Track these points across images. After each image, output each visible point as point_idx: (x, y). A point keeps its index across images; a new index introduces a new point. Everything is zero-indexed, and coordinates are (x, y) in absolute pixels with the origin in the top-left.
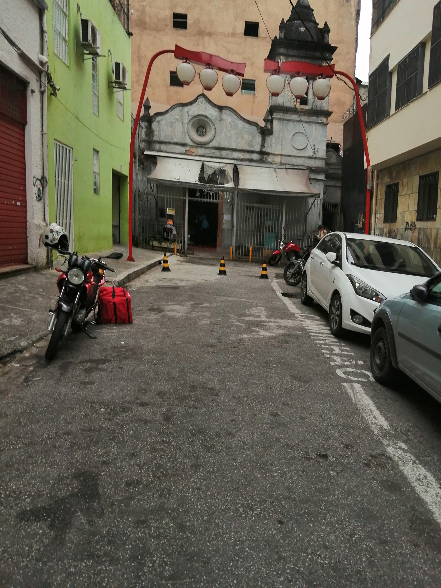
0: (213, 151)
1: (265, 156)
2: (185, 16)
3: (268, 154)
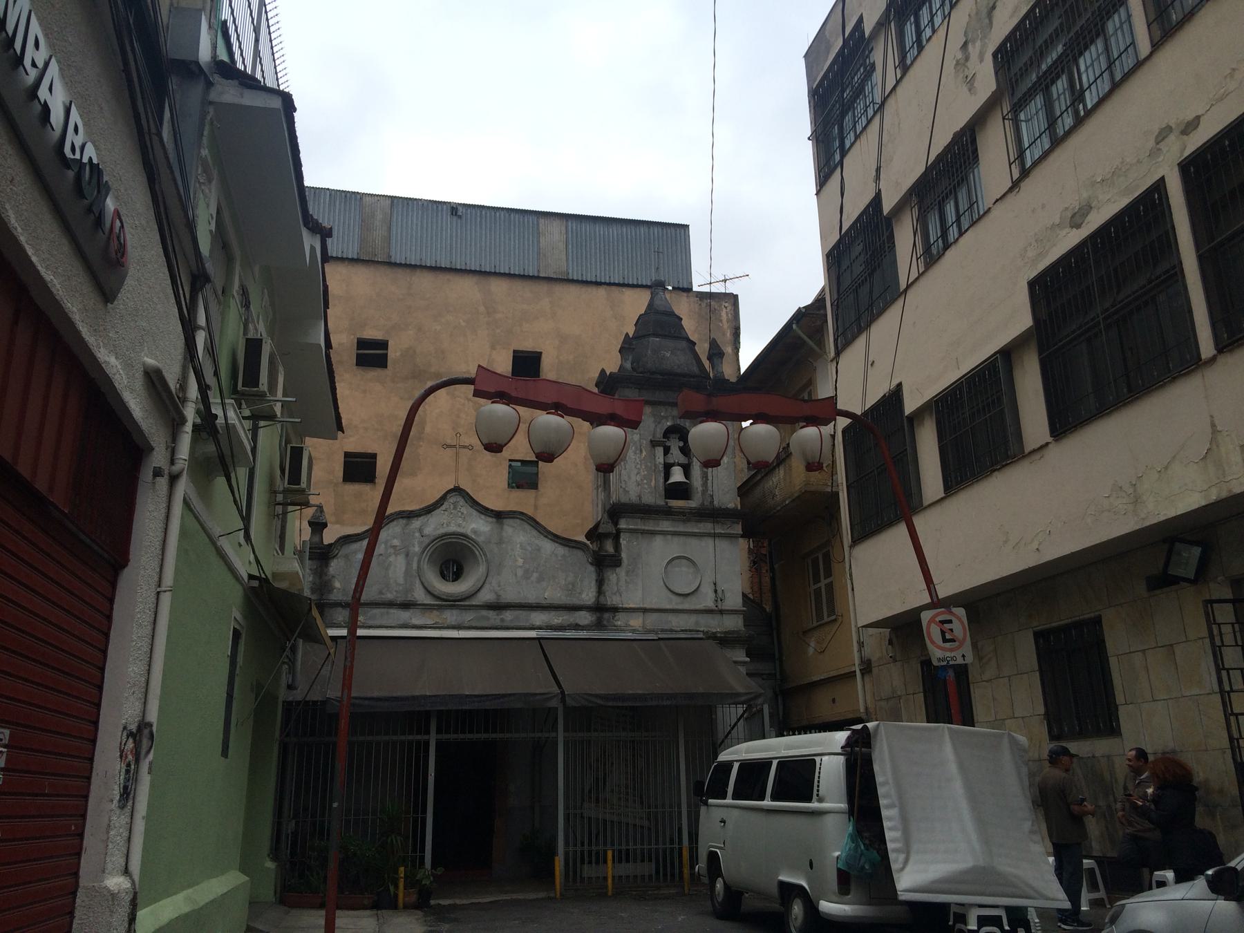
0: (484, 613)
1: (606, 615)
2: (383, 345)
3: (615, 610)
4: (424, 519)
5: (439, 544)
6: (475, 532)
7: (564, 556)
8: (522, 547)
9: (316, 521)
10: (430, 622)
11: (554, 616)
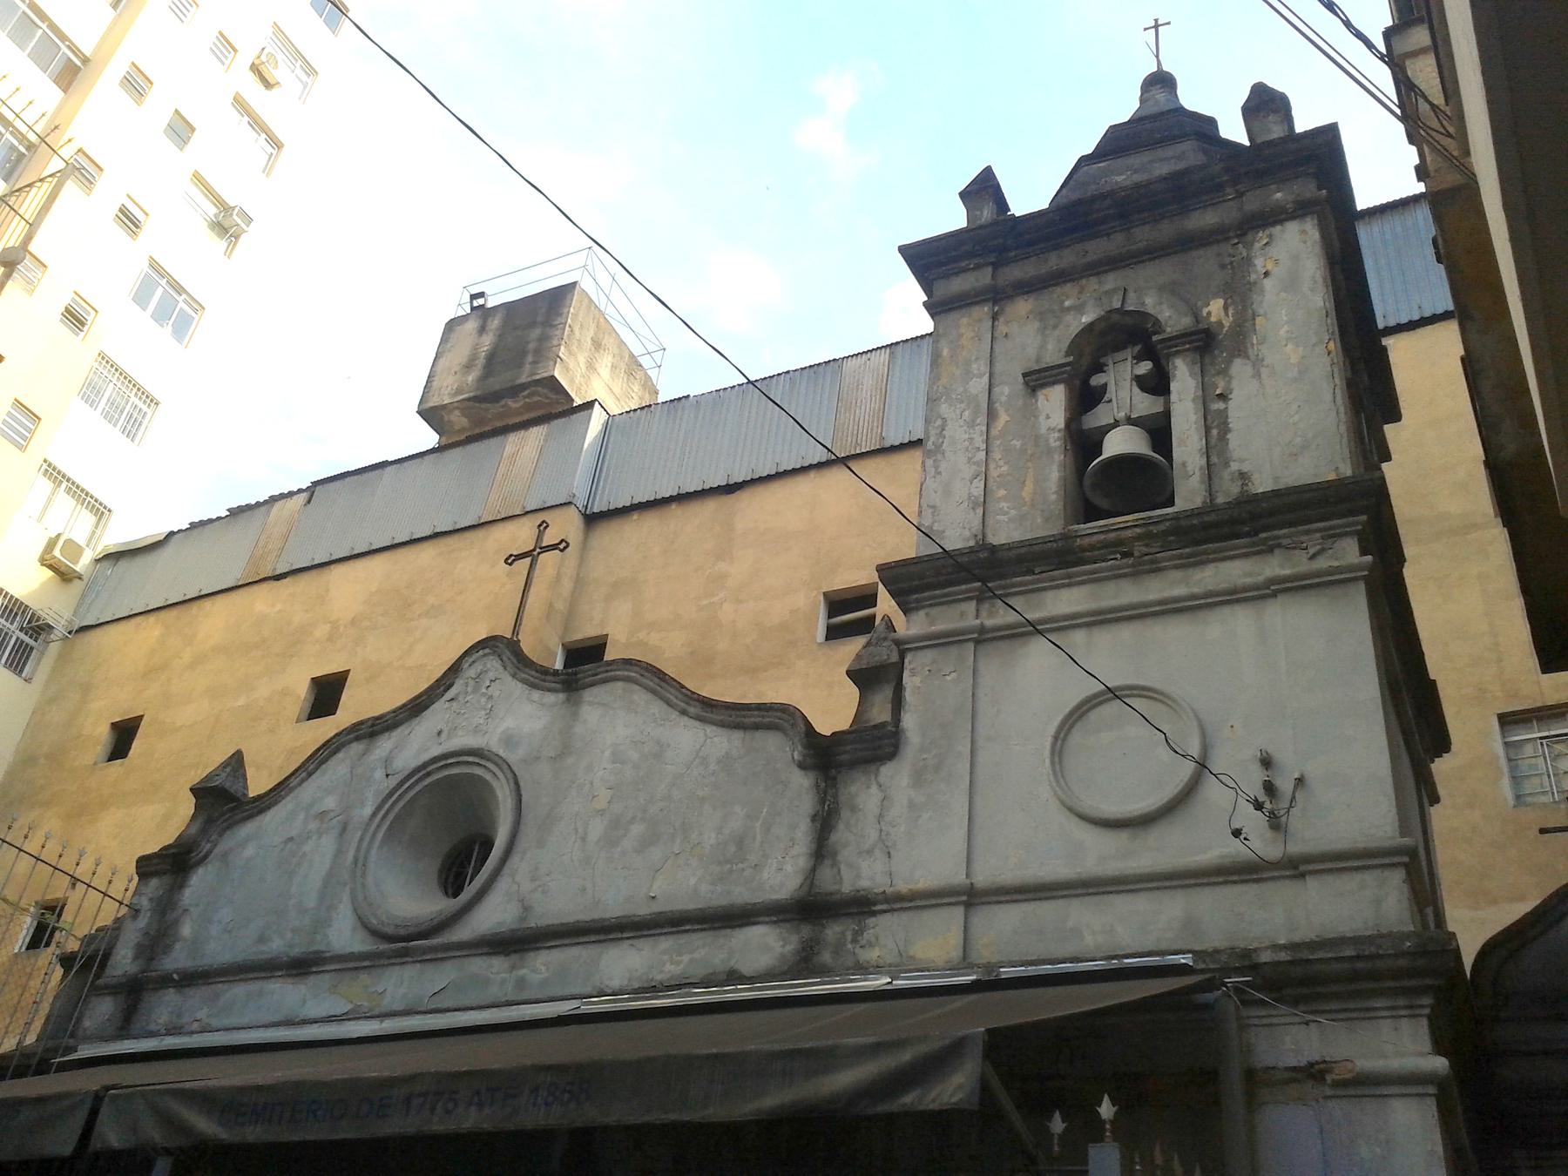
0: (479, 965)
1: (833, 931)
3: (862, 906)
5: (417, 788)
6: (509, 740)
7: (726, 761)
8: (617, 758)
10: (341, 1007)
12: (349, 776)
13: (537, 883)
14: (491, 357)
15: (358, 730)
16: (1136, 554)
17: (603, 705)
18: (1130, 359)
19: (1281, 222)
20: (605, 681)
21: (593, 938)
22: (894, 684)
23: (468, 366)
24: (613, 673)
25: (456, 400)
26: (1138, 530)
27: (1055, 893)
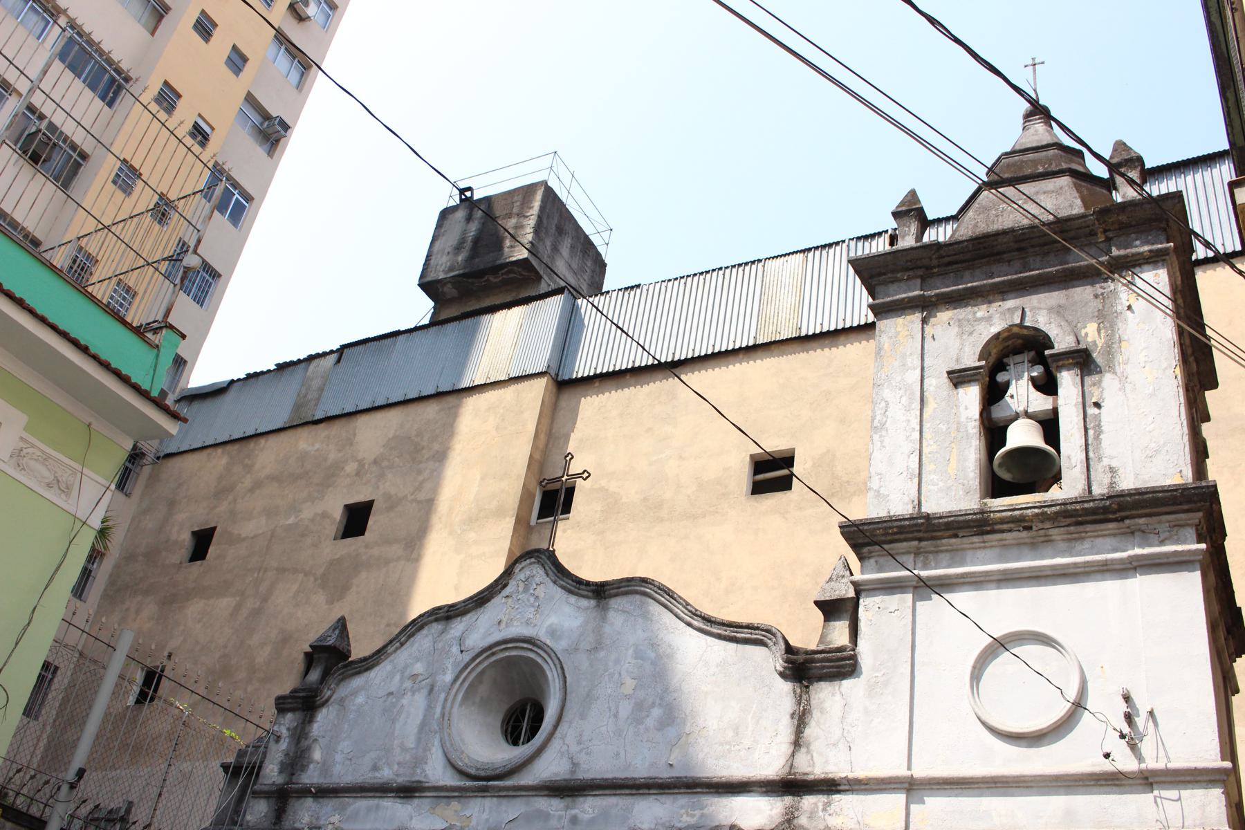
3: (829, 786)
4: (471, 618)
5: (486, 663)
6: (552, 632)
9: (320, 643)
11: (682, 807)
12: (432, 648)
13: (582, 746)
14: (477, 241)
15: (437, 614)
16: (1034, 528)
17: (624, 612)
18: (1026, 361)
19: (1140, 265)
20: (626, 593)
21: (627, 792)
22: (850, 613)
23: (458, 248)
24: (633, 588)
25: (449, 276)
26: (1036, 511)
27: (973, 786)
